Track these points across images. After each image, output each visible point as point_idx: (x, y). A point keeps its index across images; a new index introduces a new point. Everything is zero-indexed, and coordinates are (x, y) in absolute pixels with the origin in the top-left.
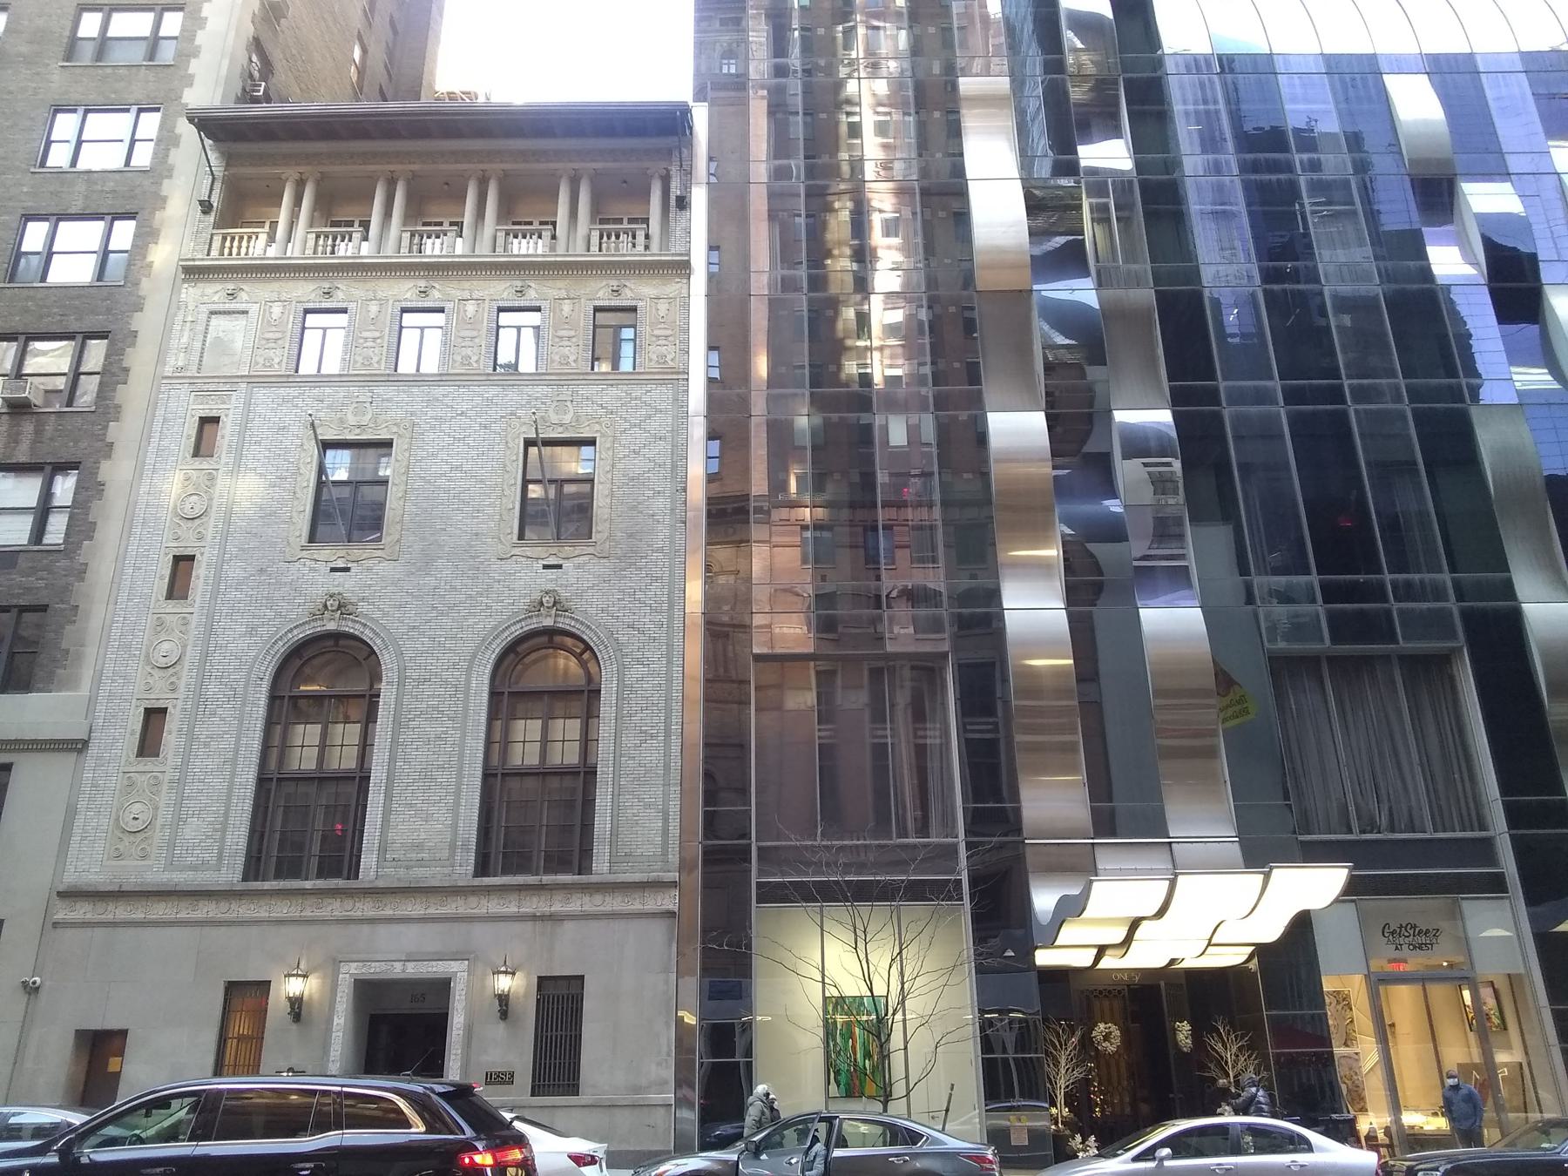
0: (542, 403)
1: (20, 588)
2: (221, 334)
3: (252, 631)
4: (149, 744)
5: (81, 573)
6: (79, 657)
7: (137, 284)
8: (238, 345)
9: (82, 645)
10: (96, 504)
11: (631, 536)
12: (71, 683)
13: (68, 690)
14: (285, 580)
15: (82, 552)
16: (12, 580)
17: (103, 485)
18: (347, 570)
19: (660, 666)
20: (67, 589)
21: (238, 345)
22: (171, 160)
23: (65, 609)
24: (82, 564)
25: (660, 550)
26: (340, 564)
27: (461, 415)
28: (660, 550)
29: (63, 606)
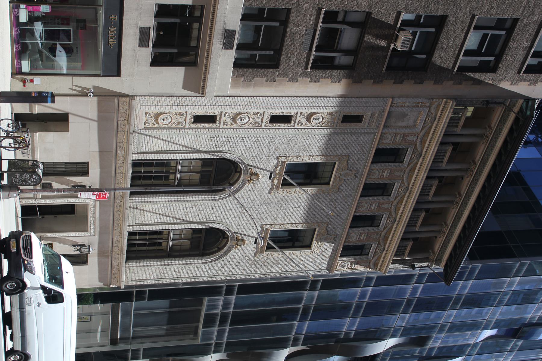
0: (333, 232)
1: (290, 55)
2: (408, 116)
3: (248, 149)
4: (199, 119)
5: (294, 80)
6: (248, 86)
7: (451, 80)
8: (400, 124)
9: (254, 87)
10: (329, 80)
11: (264, 263)
12: (235, 84)
13: (232, 84)
14: (270, 158)
15: (305, 79)
16: (296, 51)
17: (339, 82)
18: (270, 178)
19: (207, 274)
20: (286, 75)
21: (400, 124)
22: (522, 83)
23: (274, 76)
24: (298, 80)
25: (256, 270)
26: (273, 176)
27: (336, 208)
28: (256, 270)
29: (277, 75)
